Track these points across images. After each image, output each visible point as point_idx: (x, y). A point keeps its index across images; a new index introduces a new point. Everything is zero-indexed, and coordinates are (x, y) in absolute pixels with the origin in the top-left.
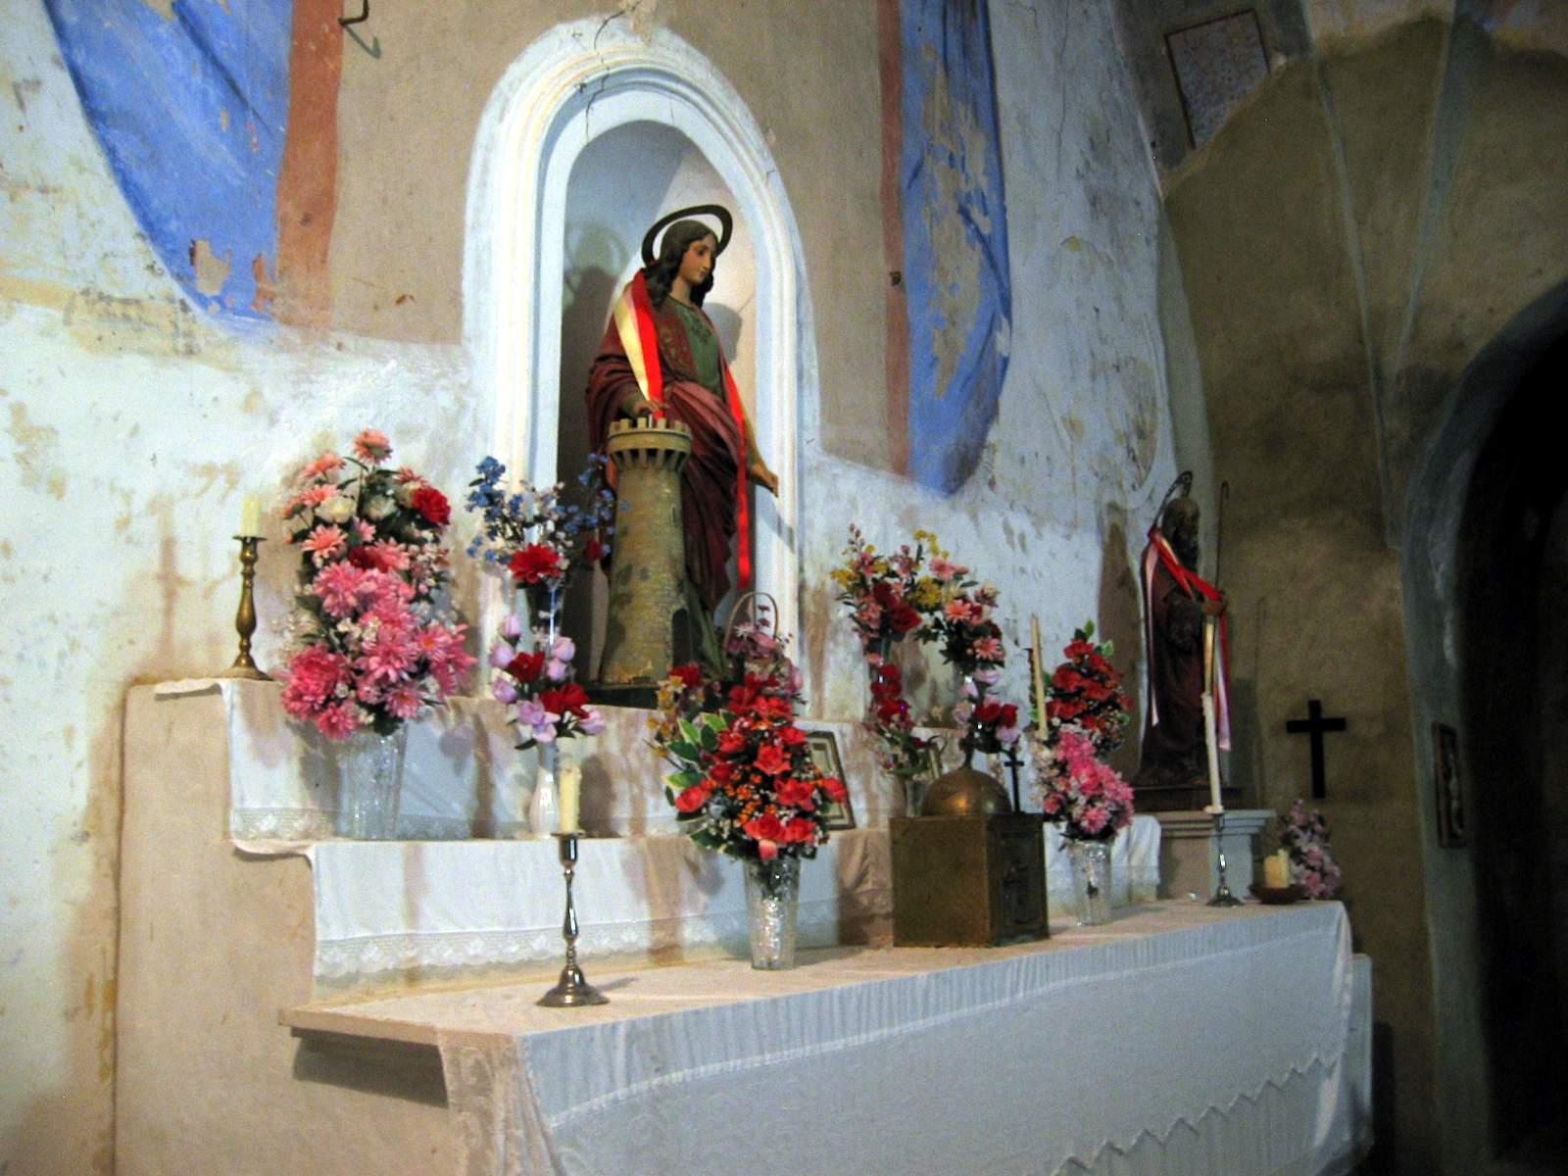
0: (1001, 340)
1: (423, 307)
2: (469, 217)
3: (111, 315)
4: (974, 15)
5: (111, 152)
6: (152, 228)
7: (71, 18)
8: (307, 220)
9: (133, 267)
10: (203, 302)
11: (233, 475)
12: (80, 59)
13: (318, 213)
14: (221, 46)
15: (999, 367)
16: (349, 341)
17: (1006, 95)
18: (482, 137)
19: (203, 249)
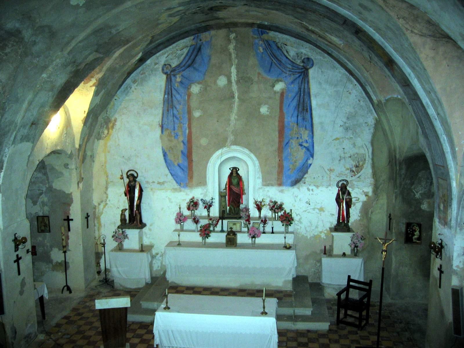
0: (310, 162)
1: (203, 182)
2: (207, 173)
3: (175, 190)
4: (307, 111)
5: (174, 178)
6: (177, 182)
7: (170, 169)
8: (191, 178)
9: (176, 186)
10: (182, 187)
11: (185, 200)
12: (171, 171)
13: (191, 177)
14: (182, 167)
15: (309, 166)
16: (195, 187)
17: (316, 120)
18: (208, 166)
19: (181, 183)
